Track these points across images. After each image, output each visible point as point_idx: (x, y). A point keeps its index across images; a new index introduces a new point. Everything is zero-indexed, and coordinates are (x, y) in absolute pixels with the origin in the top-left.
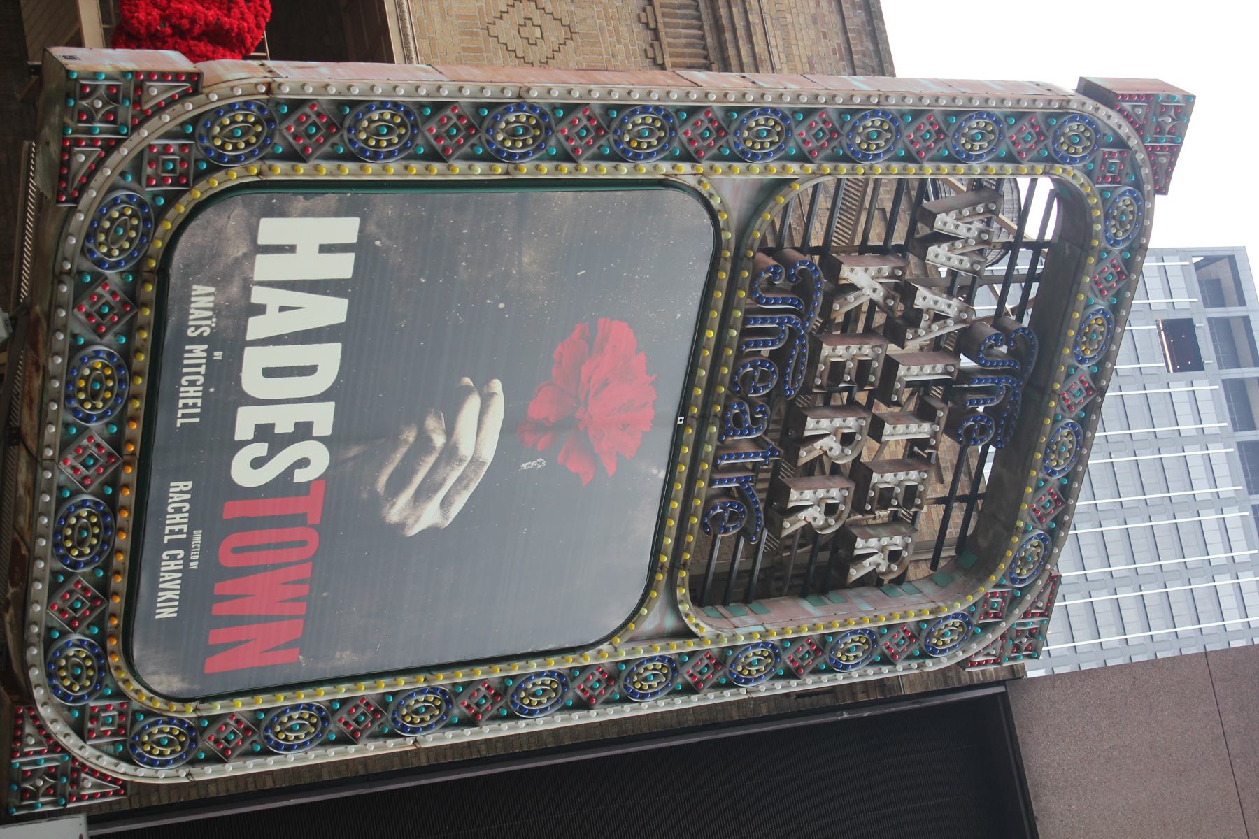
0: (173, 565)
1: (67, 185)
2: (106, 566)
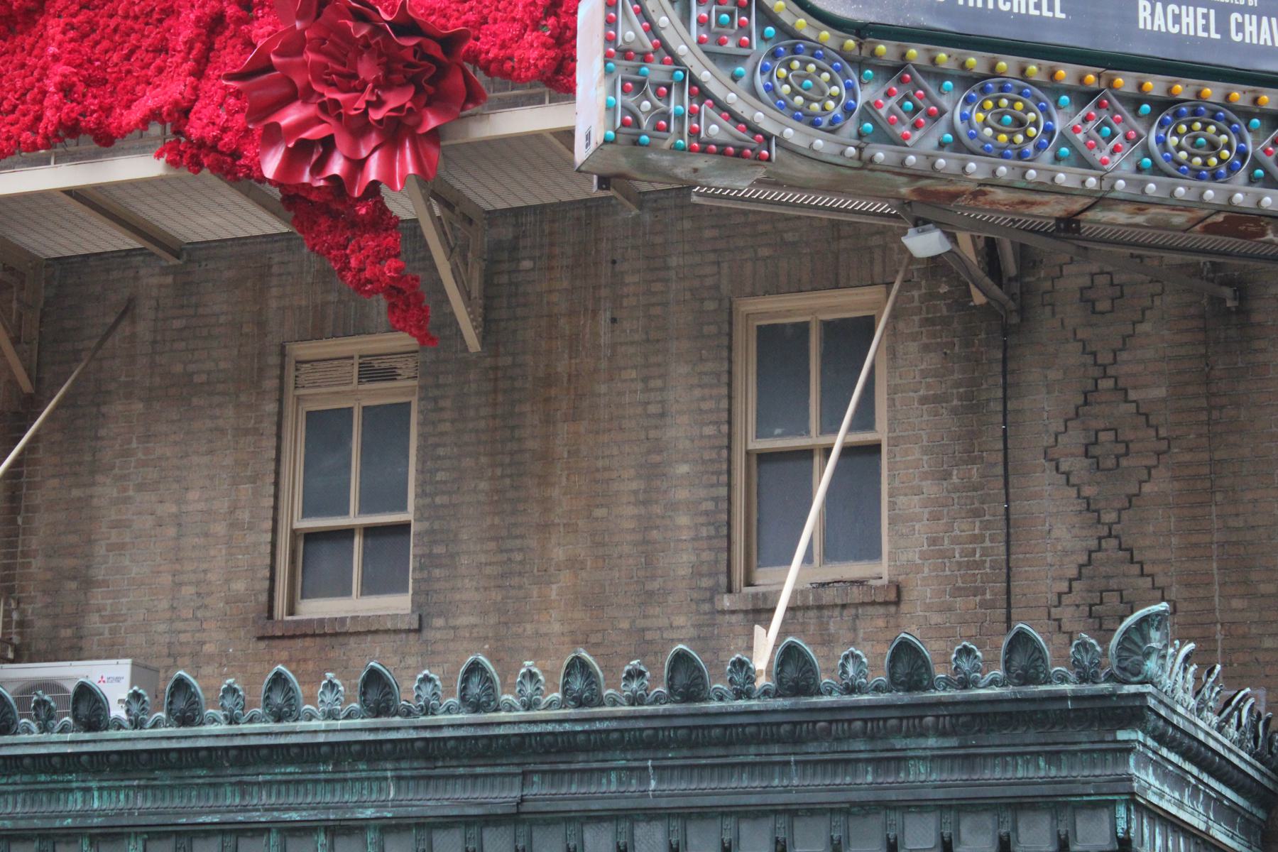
0: (1251, 28)
1: (750, 148)
2: (1246, 115)
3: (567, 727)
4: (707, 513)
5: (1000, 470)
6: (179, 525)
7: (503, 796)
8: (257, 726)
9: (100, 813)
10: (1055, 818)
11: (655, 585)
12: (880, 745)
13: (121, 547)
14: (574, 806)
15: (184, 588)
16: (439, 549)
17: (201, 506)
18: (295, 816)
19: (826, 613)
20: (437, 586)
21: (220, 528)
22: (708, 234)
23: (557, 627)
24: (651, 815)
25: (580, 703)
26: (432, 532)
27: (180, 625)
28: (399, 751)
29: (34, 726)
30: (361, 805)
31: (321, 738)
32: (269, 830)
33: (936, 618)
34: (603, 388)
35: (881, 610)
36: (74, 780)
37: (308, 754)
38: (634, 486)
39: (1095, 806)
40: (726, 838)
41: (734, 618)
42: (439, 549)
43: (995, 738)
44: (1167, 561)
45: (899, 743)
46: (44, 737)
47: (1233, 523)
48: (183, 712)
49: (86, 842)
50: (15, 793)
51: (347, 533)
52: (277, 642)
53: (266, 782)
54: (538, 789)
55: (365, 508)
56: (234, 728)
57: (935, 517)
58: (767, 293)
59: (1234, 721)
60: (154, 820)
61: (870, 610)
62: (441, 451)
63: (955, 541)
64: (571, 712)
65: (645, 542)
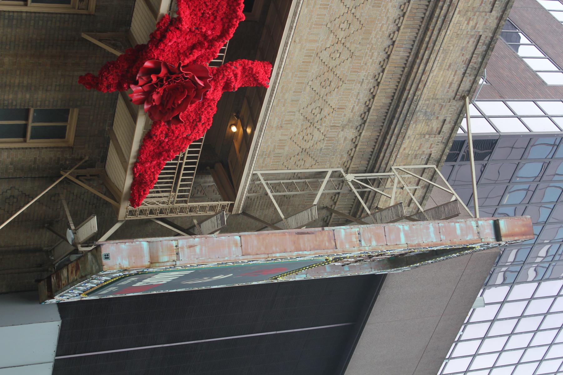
4: (12, 103)
5: (10, 177)
16: (15, 22)
22: (102, 102)
34: (59, 73)
38: (25, 82)
42: (15, 22)
58: (79, 118)
62: (49, 22)
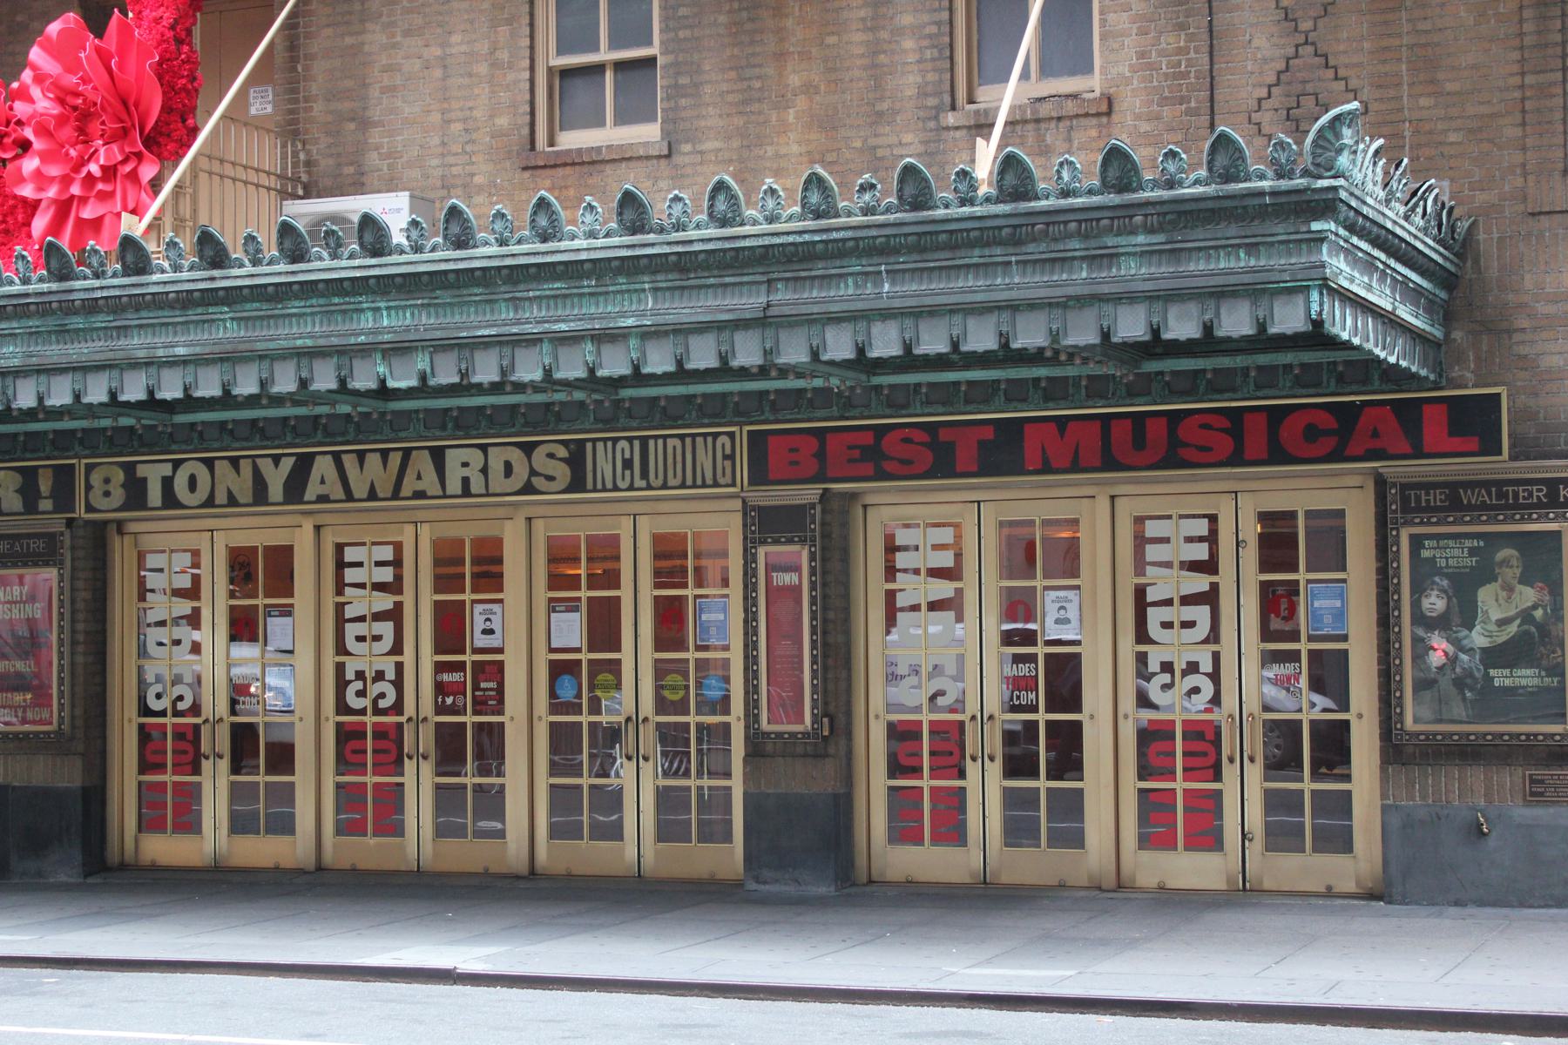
3: (807, 237)
4: (930, 36)
6: (445, 67)
7: (749, 302)
8: (525, 248)
9: (390, 330)
10: (1254, 303)
11: (885, 106)
12: (1093, 243)
13: (391, 90)
14: (816, 309)
15: (452, 126)
16: (684, 80)
17: (464, 48)
18: (563, 327)
19: (1043, 125)
20: (683, 114)
21: (483, 69)
23: (795, 149)
24: (886, 314)
25: (818, 215)
26: (675, 64)
27: (451, 160)
28: (654, 264)
29: (325, 254)
30: (623, 314)
31: (584, 256)
32: (541, 340)
33: (1145, 127)
35: (1094, 121)
36: (365, 302)
37: (572, 270)
38: (862, 13)
39: (1290, 291)
40: (955, 333)
41: (958, 134)
42: (684, 80)
43: (1199, 233)
44: (1359, 65)
45: (1110, 241)
46: (335, 263)
47: (1422, 26)
48: (458, 236)
49: (379, 356)
50: (312, 314)
51: (599, 69)
52: (539, 172)
53: (535, 298)
54: (782, 295)
55: (614, 44)
56: (505, 250)
57: (1142, 32)
59: (1420, 210)
60: (438, 334)
61: (1084, 121)
63: (1161, 53)
64: (810, 224)
65: (874, 66)
